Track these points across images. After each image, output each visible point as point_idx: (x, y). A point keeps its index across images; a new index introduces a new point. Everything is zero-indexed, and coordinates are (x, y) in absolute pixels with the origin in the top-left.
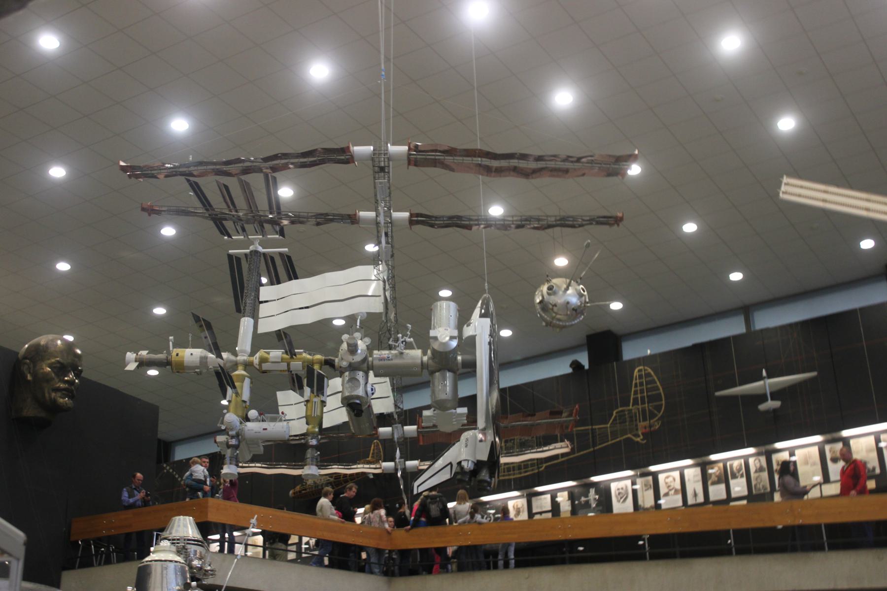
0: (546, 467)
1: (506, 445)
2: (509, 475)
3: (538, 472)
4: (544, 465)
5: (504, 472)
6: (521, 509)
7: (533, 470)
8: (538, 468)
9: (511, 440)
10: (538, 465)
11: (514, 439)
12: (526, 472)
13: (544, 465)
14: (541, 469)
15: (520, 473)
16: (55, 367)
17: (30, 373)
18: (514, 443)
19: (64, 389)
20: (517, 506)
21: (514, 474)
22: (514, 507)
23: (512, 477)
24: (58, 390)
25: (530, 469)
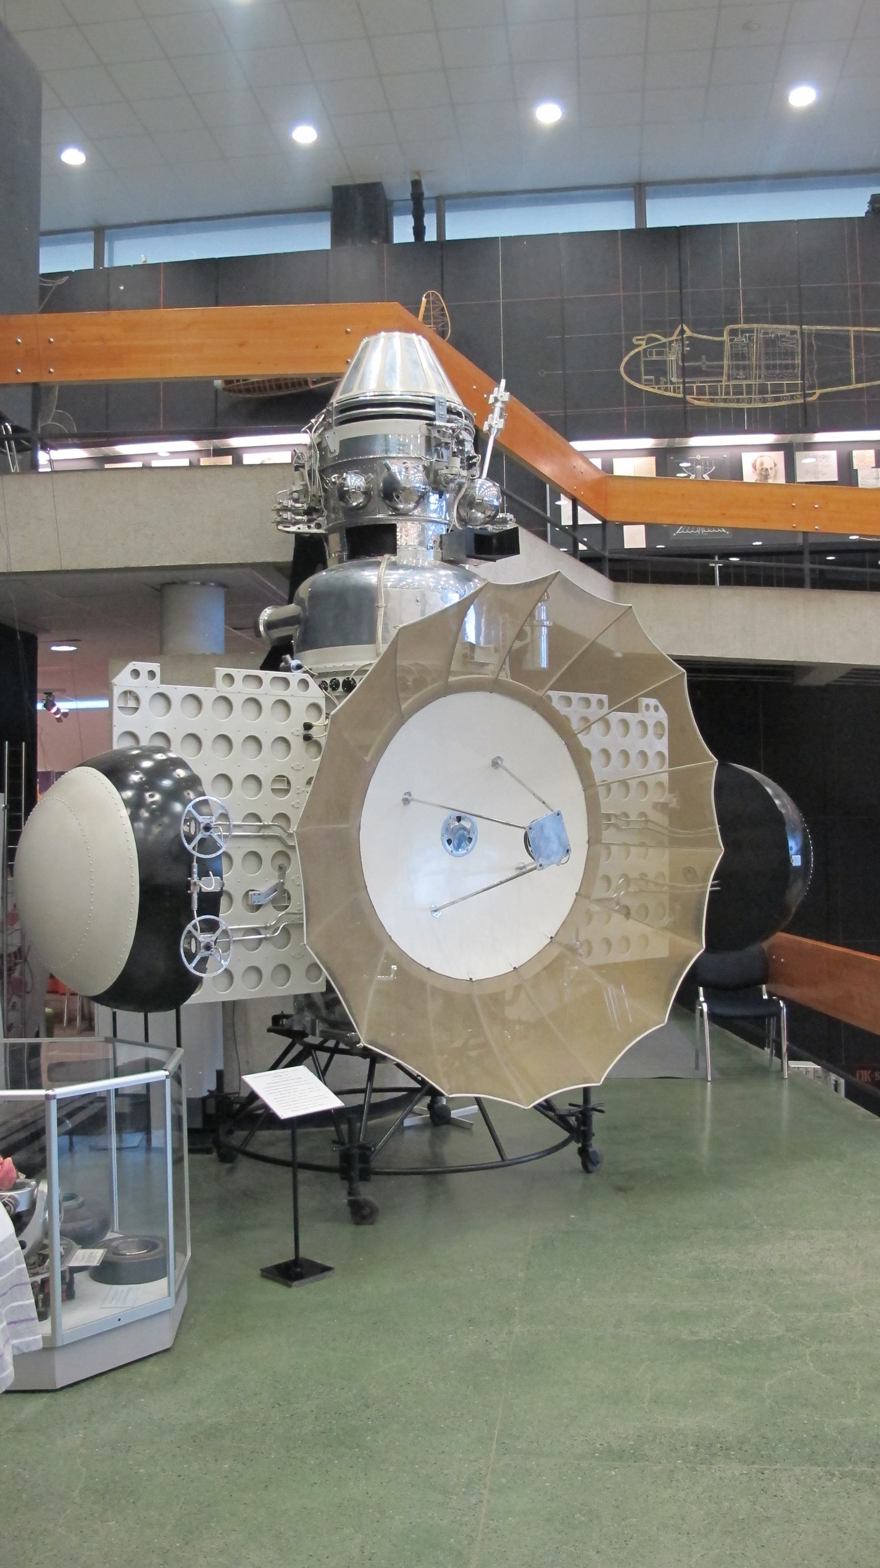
0: (822, 396)
1: (731, 340)
2: (738, 401)
3: (804, 405)
4: (819, 392)
5: (727, 393)
6: (771, 473)
7: (792, 397)
8: (805, 396)
9: (744, 331)
10: (803, 390)
11: (751, 331)
12: (777, 399)
13: (819, 392)
14: (809, 399)
15: (764, 401)
20: (762, 464)
21: (750, 401)
23: (745, 406)
25: (707, 397)
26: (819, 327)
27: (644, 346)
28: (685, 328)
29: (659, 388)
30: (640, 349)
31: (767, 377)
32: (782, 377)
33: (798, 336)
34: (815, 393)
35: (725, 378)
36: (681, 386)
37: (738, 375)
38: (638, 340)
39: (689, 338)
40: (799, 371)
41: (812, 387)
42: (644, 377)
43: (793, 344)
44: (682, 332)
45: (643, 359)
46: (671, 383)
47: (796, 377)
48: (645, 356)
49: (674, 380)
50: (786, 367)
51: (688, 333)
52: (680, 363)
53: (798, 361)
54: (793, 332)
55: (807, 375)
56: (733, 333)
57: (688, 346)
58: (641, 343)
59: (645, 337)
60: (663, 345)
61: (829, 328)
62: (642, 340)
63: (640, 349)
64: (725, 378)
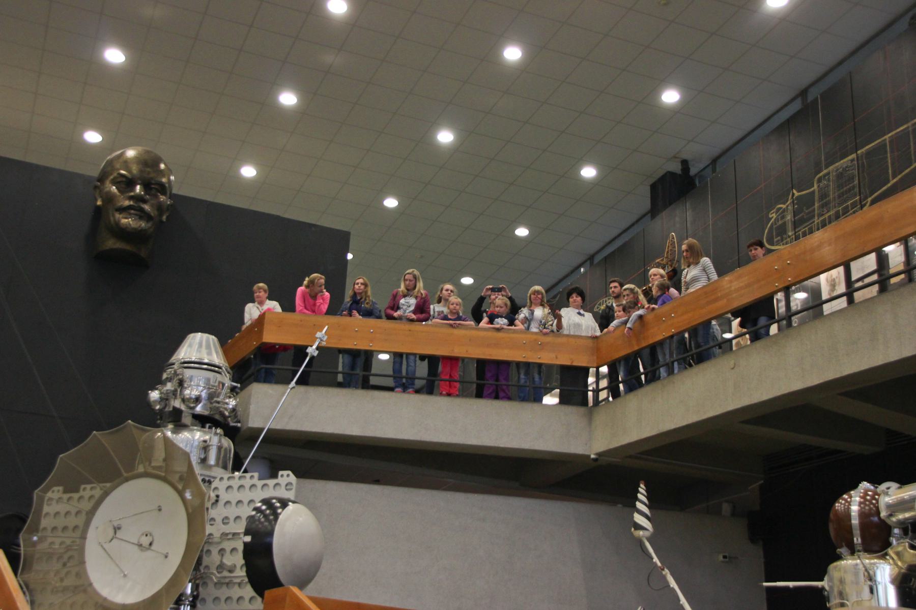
6: (837, 281)
9: (825, 176)
16: (119, 182)
17: (101, 197)
18: (829, 180)
19: (130, 208)
22: (827, 280)
24: (122, 210)
26: (867, 147)
27: (775, 217)
28: (795, 191)
29: (783, 244)
30: (773, 220)
31: (840, 204)
32: (846, 201)
33: (856, 163)
34: (867, 202)
35: (816, 218)
36: (794, 236)
37: (823, 211)
38: (772, 214)
39: (798, 198)
40: (857, 190)
41: (866, 198)
42: (775, 240)
43: (852, 170)
44: (793, 194)
45: (774, 227)
46: (789, 237)
47: (855, 196)
48: (776, 224)
49: (790, 234)
50: (850, 190)
51: (796, 194)
52: (793, 220)
53: (856, 182)
54: (852, 160)
55: (862, 190)
56: (819, 180)
57: (797, 204)
58: (773, 216)
59: (775, 210)
60: (784, 211)
61: (873, 144)
62: (773, 213)
63: (774, 218)
64: (816, 218)
